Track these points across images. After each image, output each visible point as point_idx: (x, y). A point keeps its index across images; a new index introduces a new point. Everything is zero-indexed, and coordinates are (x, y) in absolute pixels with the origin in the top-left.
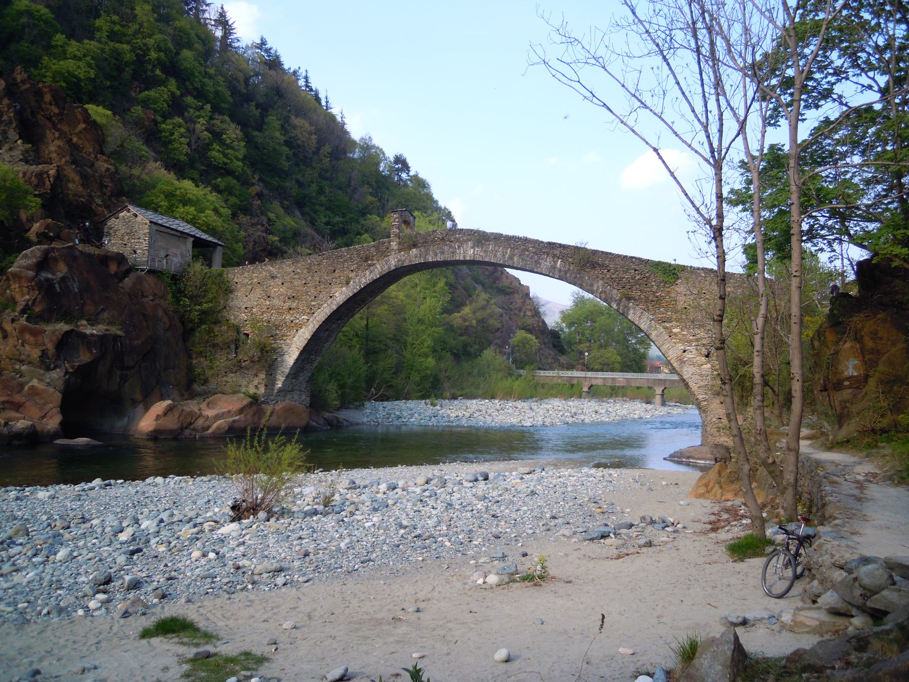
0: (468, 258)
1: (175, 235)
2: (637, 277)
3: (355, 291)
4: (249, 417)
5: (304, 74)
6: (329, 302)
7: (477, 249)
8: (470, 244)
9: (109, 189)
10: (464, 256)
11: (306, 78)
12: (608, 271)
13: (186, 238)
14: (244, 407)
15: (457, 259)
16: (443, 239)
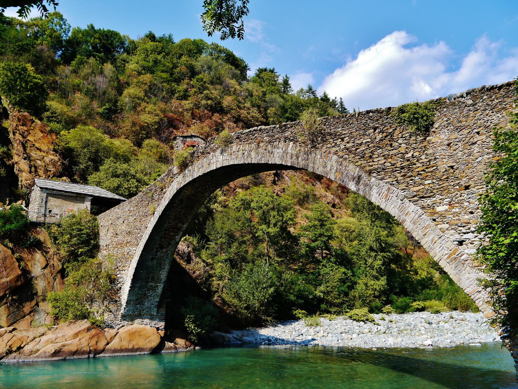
1: (71, 196)
5: (339, 101)
8: (219, 151)
9: (52, 172)
10: (216, 164)
12: (343, 140)
13: (84, 198)
14: (79, 332)
16: (203, 152)
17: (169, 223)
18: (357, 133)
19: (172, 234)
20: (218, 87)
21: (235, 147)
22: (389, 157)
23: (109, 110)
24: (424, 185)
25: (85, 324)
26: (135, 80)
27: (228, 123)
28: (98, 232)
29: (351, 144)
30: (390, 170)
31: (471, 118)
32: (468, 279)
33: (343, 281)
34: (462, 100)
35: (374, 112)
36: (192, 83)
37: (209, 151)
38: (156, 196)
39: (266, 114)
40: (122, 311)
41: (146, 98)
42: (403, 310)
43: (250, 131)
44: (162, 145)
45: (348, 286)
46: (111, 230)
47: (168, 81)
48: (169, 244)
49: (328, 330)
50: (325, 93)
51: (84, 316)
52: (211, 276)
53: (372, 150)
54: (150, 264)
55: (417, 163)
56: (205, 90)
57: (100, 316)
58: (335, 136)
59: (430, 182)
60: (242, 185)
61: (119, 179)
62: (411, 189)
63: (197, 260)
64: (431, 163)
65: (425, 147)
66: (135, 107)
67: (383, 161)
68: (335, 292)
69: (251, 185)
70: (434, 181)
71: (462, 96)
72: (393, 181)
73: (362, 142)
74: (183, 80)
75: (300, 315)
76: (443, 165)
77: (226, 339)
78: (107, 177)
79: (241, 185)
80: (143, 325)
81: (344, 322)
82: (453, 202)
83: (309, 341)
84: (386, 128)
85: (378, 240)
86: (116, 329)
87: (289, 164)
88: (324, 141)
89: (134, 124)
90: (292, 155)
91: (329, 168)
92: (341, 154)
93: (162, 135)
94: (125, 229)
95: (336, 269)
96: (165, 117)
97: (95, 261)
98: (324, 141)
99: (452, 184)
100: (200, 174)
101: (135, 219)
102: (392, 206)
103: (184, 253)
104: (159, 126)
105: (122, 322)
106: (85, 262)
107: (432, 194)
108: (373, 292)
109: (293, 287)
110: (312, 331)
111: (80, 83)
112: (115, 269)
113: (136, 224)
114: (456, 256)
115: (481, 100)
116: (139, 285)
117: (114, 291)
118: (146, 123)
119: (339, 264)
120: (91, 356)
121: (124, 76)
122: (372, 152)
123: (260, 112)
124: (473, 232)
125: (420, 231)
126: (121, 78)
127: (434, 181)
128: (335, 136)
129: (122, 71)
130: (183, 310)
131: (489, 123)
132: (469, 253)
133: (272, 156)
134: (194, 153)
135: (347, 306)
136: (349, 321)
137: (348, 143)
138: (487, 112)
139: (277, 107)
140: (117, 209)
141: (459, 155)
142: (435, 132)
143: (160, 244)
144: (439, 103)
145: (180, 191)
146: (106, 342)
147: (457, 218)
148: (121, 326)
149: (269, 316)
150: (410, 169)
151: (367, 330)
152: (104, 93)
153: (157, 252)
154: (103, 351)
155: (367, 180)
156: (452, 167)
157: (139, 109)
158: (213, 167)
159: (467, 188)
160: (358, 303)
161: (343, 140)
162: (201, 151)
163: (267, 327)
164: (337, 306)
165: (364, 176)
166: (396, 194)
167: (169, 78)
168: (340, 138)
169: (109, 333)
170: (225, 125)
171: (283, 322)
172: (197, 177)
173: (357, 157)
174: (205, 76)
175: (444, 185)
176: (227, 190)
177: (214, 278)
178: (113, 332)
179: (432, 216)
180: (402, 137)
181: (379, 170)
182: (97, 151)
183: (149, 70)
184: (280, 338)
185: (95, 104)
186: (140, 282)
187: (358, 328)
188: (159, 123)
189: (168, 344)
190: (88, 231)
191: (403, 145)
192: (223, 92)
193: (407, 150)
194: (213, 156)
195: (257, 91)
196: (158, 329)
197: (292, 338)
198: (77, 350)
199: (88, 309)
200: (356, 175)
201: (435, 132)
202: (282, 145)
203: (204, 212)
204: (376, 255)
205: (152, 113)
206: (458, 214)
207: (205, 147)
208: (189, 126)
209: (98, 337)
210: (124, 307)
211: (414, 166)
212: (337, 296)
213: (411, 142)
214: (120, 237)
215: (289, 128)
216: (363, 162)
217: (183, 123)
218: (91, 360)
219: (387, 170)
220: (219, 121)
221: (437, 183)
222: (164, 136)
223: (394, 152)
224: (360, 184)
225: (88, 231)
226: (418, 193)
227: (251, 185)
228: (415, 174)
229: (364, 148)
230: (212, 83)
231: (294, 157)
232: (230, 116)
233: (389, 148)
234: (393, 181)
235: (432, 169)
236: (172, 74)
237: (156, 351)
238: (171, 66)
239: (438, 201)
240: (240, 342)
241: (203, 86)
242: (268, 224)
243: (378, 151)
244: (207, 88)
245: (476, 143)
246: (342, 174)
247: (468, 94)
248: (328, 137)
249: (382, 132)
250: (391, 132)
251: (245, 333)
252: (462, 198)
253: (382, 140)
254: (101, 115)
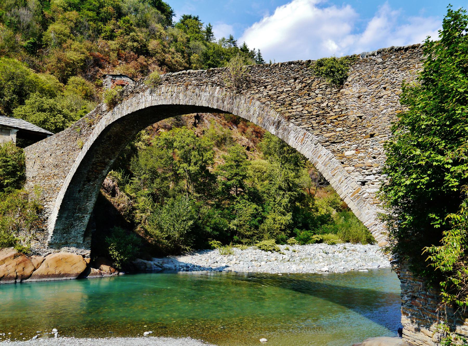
4: (10, 267)
5: (257, 52)
8: (148, 91)
10: (145, 104)
11: (259, 54)
13: (10, 130)
14: (6, 259)
16: (133, 92)
17: (97, 158)
18: (279, 82)
19: (99, 168)
20: (144, 30)
21: (163, 88)
22: (307, 105)
23: (34, 44)
24: (336, 132)
25: (12, 251)
26: (61, 16)
27: (153, 66)
28: (25, 164)
29: (273, 92)
30: (307, 117)
31: (380, 75)
32: (368, 213)
33: (254, 216)
34: (373, 58)
35: (296, 64)
36: (118, 23)
37: (138, 91)
38: (85, 131)
39: (189, 59)
40: (49, 239)
41: (72, 35)
42: (305, 241)
43: (179, 74)
44: (87, 83)
45: (259, 220)
46: (38, 163)
47: (95, 20)
48: (96, 178)
49: (240, 258)
50: (245, 44)
51: (11, 244)
52: (134, 209)
53: (291, 98)
54: (77, 195)
55: (331, 112)
56: (131, 32)
57: (27, 244)
58: (259, 83)
59: (341, 129)
60: (165, 126)
61: (45, 113)
62: (324, 135)
63: (121, 193)
64: (343, 113)
65: (338, 98)
66: (60, 44)
67: (301, 109)
68: (247, 226)
69: (173, 126)
70: (345, 128)
71: (373, 55)
72: (308, 127)
73: (283, 91)
74: (110, 20)
75: (216, 245)
76: (353, 115)
77: (148, 266)
78: (32, 111)
79: (164, 126)
80: (70, 253)
81: (254, 251)
82: (359, 148)
83: (223, 268)
84: (305, 79)
85: (286, 180)
86: (43, 256)
87: (215, 107)
88: (248, 87)
89: (59, 60)
90: (218, 98)
91: (252, 113)
92: (263, 100)
93: (88, 73)
94: (52, 162)
95: (249, 205)
96: (91, 55)
97: (21, 192)
98: (248, 88)
99: (360, 132)
100: (129, 113)
102: (307, 149)
103: (109, 187)
104: (84, 64)
105: (49, 250)
106: (11, 192)
107: (342, 140)
108: (279, 226)
109: (210, 220)
110: (225, 259)
111: (3, 14)
112: (42, 200)
113: (63, 157)
114: (359, 194)
115: (389, 60)
116: (65, 215)
117: (41, 220)
118: (71, 60)
119: (252, 201)
120: (18, 281)
121: (49, 11)
122: (291, 100)
123: (184, 57)
124: (374, 174)
125: (330, 172)
126: (46, 13)
127: (345, 128)
128: (259, 83)
129: (47, 5)
130: (108, 239)
131: (395, 80)
132: (370, 192)
133: (199, 98)
134: (123, 92)
135: (257, 237)
136: (258, 251)
137: (270, 90)
138: (394, 70)
139: (200, 54)
140: (44, 143)
141: (367, 106)
142: (348, 85)
143: (87, 178)
144: (353, 59)
145: (108, 128)
146: (33, 268)
147: (362, 161)
148: (47, 253)
149: (187, 246)
150: (324, 117)
151: (273, 259)
152: (28, 27)
153: (84, 185)
154: (30, 276)
155: (286, 125)
156: (360, 117)
157: (64, 45)
158: (142, 106)
159: (372, 136)
160: (266, 235)
161: (266, 87)
162: (131, 90)
163: (185, 256)
164: (248, 238)
165: (284, 121)
166: (311, 139)
167: (96, 17)
168: (264, 86)
169: (36, 260)
170: (150, 68)
171: (199, 251)
172: (126, 115)
173: (278, 104)
174: (132, 18)
175: (352, 133)
176: (150, 130)
177: (137, 211)
178: (40, 259)
179: (341, 159)
180: (319, 88)
181: (297, 117)
182: (22, 85)
183: (75, 7)
184: (197, 265)
185: (19, 37)
186: (67, 212)
187: (266, 256)
188: (85, 61)
189: (93, 270)
190: (14, 162)
191: (319, 95)
192: (149, 35)
193: (323, 100)
194: (142, 96)
195: (181, 37)
196: (84, 256)
197: (208, 265)
198: (4, 276)
199: (14, 237)
200: (276, 120)
201: (348, 85)
202: (209, 88)
203: (128, 150)
204: (284, 194)
205: (78, 51)
206: (363, 158)
207: (135, 87)
208: (114, 66)
209: (25, 264)
210: (51, 235)
211: (328, 115)
212: (249, 229)
213: (327, 93)
214: (47, 170)
215: (216, 73)
216: (283, 109)
217: (109, 63)
218: (18, 285)
219: (304, 117)
220: (145, 63)
221: (347, 130)
222: (90, 74)
223: (312, 101)
224: (280, 128)
225: (14, 162)
226: (330, 139)
227: (173, 126)
228: (328, 121)
229: (284, 96)
230: (138, 25)
231: (220, 101)
232: (155, 59)
233: (307, 97)
234: (308, 127)
235: (343, 118)
236: (98, 14)
237: (82, 277)
238: (98, 5)
239: (347, 146)
240: (160, 269)
241: (129, 28)
242: (189, 163)
243: (297, 99)
244: (133, 30)
245: (382, 97)
246: (264, 118)
247: (378, 53)
248: (252, 84)
249: (301, 82)
250: (310, 83)
251: (166, 260)
252: (367, 144)
253: (301, 90)
254: (25, 48)
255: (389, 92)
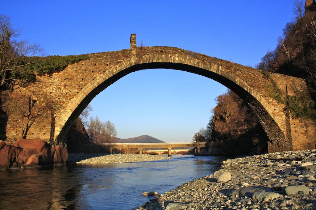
0: (176, 62)
2: (253, 77)
3: (110, 76)
6: (92, 82)
7: (180, 58)
10: (174, 61)
15: (170, 62)
100: (160, 62)
101: (76, 71)
255: (281, 86)
